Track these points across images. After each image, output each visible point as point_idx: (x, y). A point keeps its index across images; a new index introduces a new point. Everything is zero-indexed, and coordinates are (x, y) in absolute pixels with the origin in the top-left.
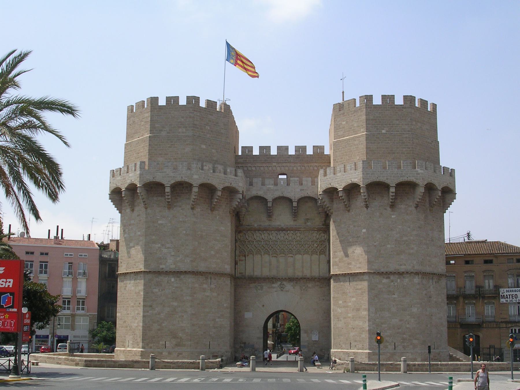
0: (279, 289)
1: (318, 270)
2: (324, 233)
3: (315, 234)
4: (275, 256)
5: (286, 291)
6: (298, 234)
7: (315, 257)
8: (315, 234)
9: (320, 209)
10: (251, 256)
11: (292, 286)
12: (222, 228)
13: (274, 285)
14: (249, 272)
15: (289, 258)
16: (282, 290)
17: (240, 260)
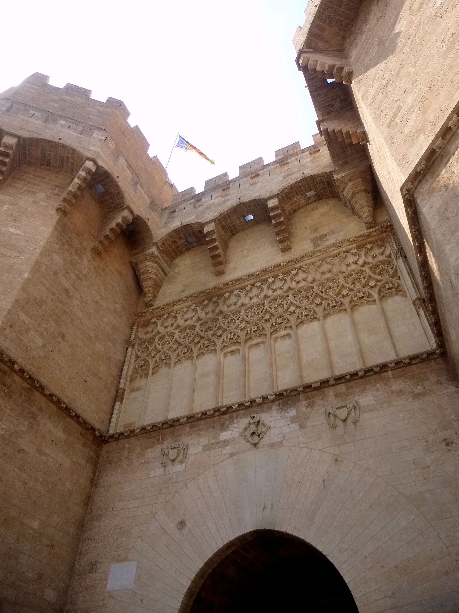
0: (243, 444)
1: (387, 344)
2: (380, 246)
3: (351, 259)
4: (232, 352)
5: (272, 445)
6: (301, 276)
7: (367, 312)
8: (351, 259)
9: (345, 193)
10: (164, 370)
11: (293, 420)
12: (12, 230)
13: (224, 436)
14: (152, 416)
15: (279, 342)
16: (255, 445)
17: (133, 390)
